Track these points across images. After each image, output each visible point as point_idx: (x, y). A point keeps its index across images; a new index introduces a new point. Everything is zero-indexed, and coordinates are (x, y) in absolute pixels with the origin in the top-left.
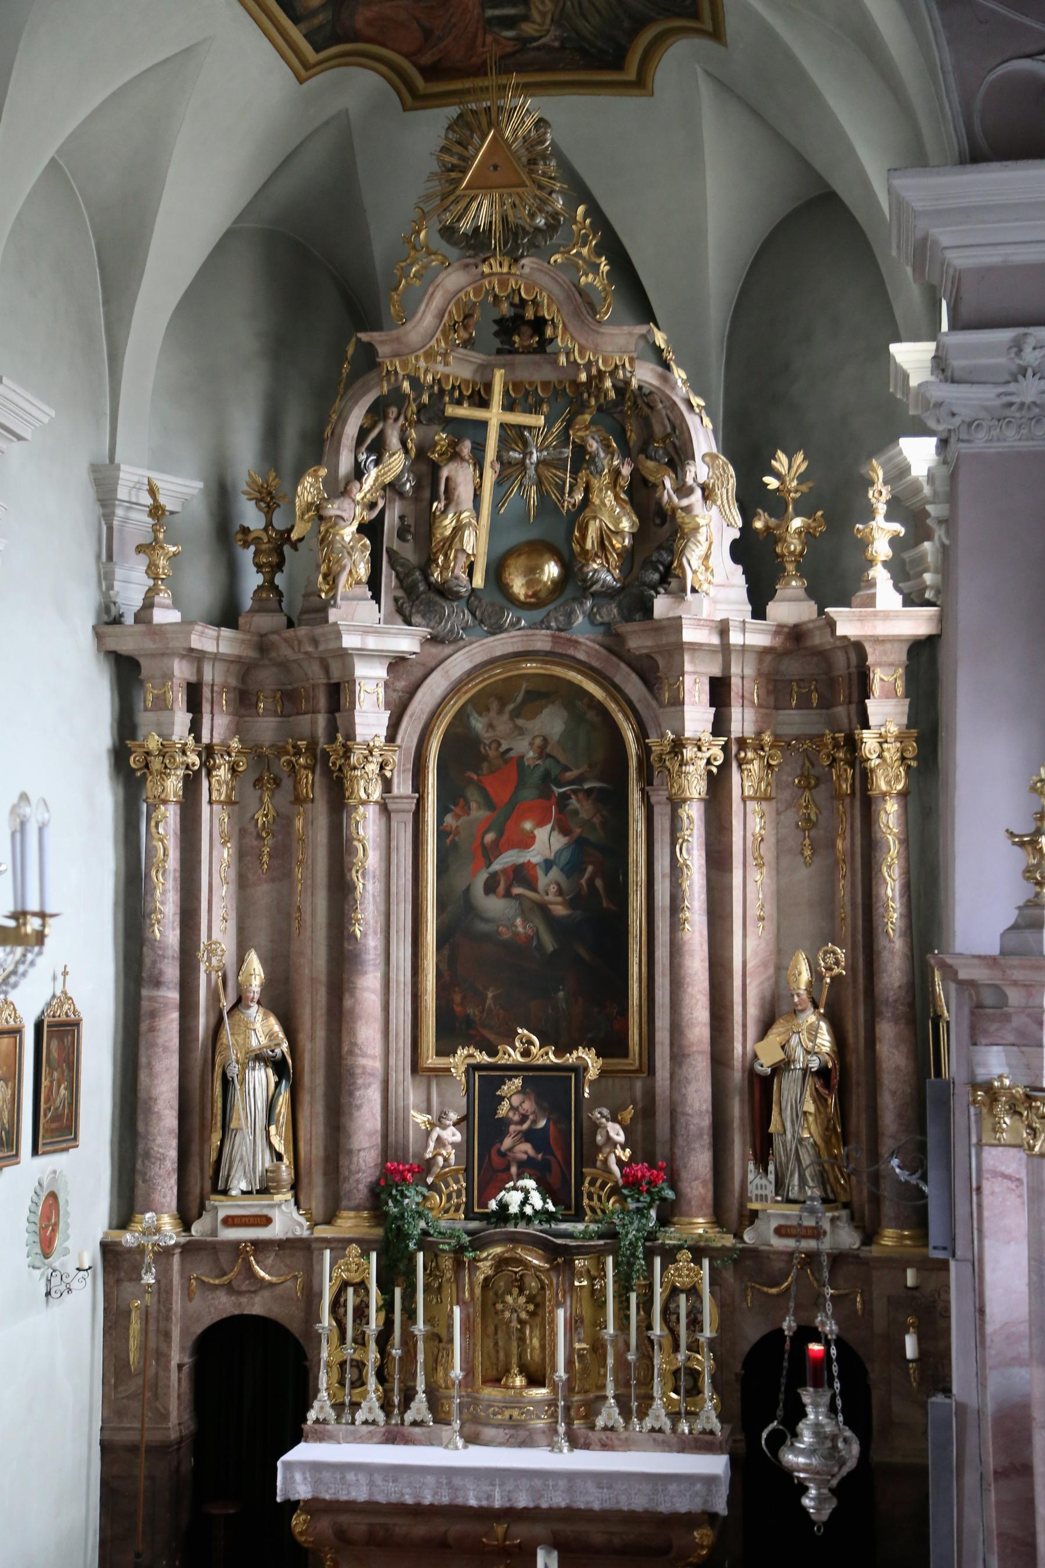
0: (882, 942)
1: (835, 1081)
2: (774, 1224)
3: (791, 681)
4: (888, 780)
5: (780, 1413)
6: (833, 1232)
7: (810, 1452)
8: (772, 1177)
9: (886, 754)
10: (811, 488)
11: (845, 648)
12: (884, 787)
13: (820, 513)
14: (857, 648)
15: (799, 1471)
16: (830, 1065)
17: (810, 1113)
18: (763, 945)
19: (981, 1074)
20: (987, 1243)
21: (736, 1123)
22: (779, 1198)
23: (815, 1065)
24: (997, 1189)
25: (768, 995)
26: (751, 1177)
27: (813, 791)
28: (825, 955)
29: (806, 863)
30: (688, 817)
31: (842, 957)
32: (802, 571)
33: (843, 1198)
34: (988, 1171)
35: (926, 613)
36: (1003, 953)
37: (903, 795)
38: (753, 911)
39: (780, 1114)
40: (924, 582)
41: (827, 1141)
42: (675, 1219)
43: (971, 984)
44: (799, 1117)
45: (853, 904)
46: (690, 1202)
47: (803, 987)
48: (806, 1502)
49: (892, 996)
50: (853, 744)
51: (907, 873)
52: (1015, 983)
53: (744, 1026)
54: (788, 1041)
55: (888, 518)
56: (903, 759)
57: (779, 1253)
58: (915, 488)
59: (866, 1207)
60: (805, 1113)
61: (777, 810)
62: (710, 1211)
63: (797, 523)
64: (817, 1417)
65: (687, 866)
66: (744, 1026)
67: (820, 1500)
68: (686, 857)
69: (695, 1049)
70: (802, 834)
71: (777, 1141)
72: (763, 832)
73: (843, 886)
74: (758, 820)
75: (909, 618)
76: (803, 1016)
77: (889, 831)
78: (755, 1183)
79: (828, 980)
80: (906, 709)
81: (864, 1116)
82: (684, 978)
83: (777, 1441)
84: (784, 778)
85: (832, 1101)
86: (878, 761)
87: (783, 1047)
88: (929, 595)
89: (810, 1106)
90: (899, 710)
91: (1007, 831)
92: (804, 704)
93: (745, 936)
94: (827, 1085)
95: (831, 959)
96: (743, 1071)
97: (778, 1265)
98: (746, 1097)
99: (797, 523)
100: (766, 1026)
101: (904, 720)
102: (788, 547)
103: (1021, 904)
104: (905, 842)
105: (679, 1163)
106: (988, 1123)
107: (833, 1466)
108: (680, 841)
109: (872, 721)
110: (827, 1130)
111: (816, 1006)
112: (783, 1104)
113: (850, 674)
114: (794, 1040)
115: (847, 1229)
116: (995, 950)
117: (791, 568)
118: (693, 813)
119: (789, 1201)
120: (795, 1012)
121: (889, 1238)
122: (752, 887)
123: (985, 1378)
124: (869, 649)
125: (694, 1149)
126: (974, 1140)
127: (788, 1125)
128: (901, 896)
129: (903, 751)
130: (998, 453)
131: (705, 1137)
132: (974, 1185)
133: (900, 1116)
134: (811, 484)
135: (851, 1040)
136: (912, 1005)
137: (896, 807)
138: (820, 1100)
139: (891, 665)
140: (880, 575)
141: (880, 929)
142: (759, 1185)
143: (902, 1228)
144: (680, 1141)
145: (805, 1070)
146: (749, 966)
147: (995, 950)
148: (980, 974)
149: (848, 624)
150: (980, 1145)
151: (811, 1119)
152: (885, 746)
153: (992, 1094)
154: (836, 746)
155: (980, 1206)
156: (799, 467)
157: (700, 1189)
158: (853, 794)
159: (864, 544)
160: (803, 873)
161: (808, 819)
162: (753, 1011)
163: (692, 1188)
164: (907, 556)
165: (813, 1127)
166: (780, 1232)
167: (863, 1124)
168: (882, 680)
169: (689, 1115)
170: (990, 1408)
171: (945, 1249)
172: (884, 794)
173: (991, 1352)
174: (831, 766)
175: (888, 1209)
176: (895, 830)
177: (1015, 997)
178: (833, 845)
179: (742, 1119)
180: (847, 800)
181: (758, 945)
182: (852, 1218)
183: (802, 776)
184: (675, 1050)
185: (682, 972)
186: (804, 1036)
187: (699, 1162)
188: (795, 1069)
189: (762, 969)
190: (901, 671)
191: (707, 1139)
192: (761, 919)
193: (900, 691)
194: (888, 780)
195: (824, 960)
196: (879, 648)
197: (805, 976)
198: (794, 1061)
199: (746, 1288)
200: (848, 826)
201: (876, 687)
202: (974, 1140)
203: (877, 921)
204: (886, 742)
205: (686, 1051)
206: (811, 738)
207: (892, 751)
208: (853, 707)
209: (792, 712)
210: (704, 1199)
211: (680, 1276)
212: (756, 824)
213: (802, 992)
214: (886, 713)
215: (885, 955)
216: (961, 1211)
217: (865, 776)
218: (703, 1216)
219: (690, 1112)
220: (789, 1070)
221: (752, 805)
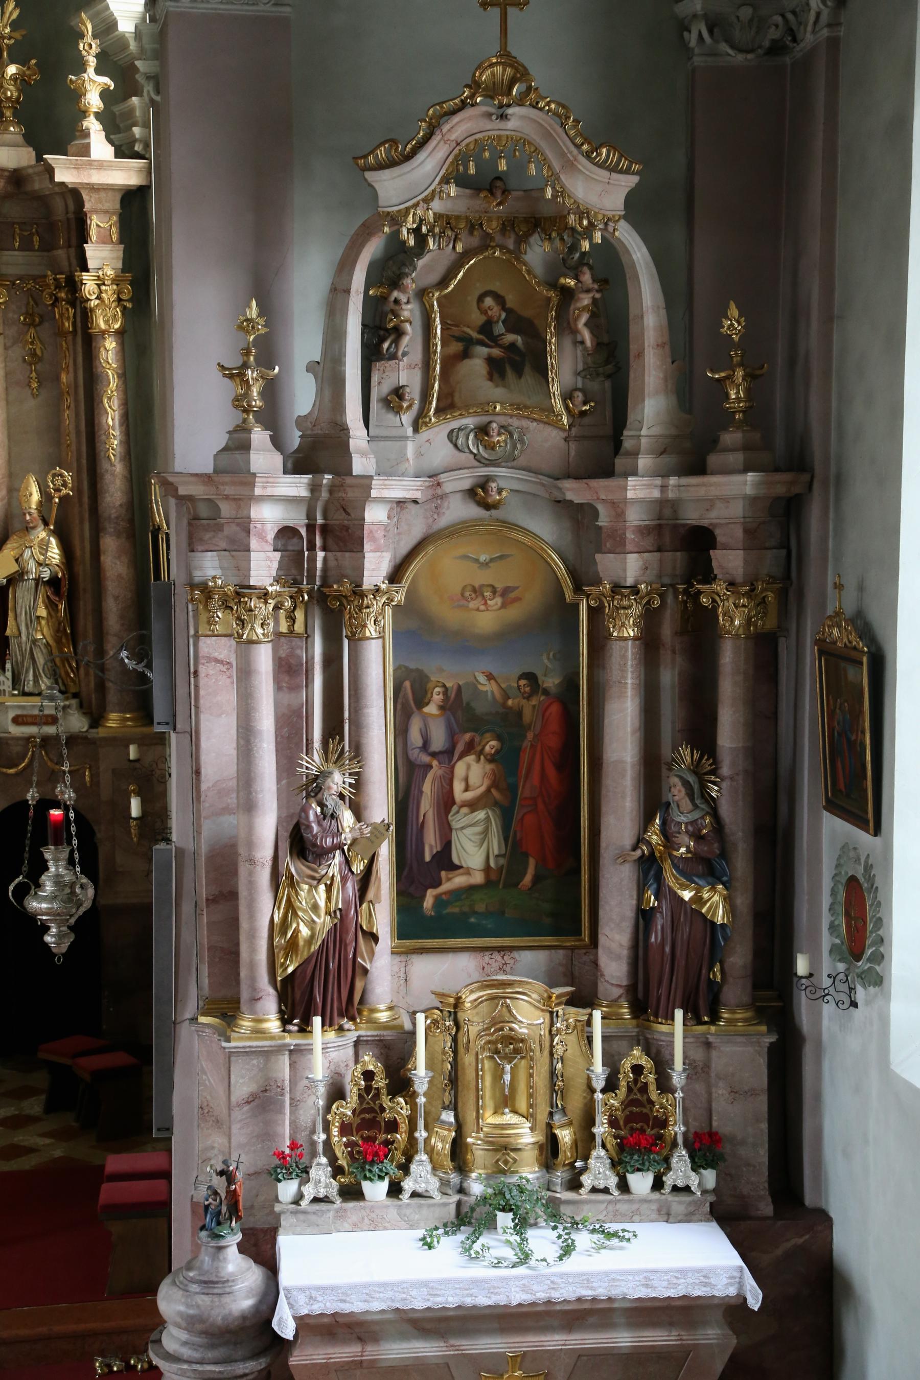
0: (105, 465)
1: (65, 589)
2: (11, 715)
3: (14, 223)
4: (107, 319)
5: (25, 869)
7: (52, 898)
8: (9, 674)
9: (104, 295)
10: (23, 36)
11: (62, 194)
12: (103, 326)
13: (33, 62)
14: (74, 194)
15: (42, 915)
16: (60, 575)
17: (43, 618)
19: (198, 576)
20: (203, 717)
22: (16, 692)
23: (46, 575)
24: (211, 672)
27: (38, 328)
29: (33, 395)
31: (69, 479)
32: (20, 118)
33: (73, 689)
34: (203, 657)
35: (136, 165)
36: (215, 471)
37: (120, 333)
39: (16, 619)
40: (134, 135)
41: (58, 641)
43: (190, 498)
45: (78, 432)
47: (34, 507)
48: (48, 939)
49: (114, 513)
50: (74, 286)
51: (125, 404)
52: (227, 497)
54: (21, 555)
55: (98, 71)
56: (119, 300)
58: (122, 41)
60: (38, 617)
61: (5, 345)
63: (12, 70)
64: (57, 869)
67: (60, 936)
70: (28, 367)
71: (13, 643)
73: (68, 416)
75: (121, 169)
76: (34, 532)
77: (108, 366)
79: (57, 500)
80: (121, 254)
83: (22, 892)
84: (11, 315)
85: (62, 607)
86: (97, 302)
87: (17, 560)
88: (138, 148)
89: (42, 612)
90: (115, 255)
91: (219, 364)
92: (26, 246)
94: (57, 592)
95: (59, 482)
97: (17, 749)
99: (12, 70)
101: (120, 265)
102: (5, 94)
103: (231, 429)
104: (123, 376)
106: (203, 617)
107: (72, 907)
109: (91, 264)
110: (58, 632)
111: (46, 524)
112: (18, 611)
113: (68, 219)
114: (27, 554)
115: (76, 715)
116: (209, 470)
117: (8, 113)
119: (25, 694)
120: (28, 529)
121: (113, 721)
123: (200, 826)
124: (85, 197)
126: (192, 632)
127: (23, 629)
128: (121, 425)
129: (119, 293)
130: (202, 13)
132: (192, 670)
133: (122, 617)
134: (24, 33)
135: (78, 553)
136: (131, 521)
137: (114, 345)
138: (51, 606)
139: (106, 212)
140: (93, 125)
141: (102, 454)
143: (125, 712)
145: (38, 580)
147: (209, 470)
148: (197, 490)
149: (65, 172)
150: (197, 636)
151: (43, 622)
152: (103, 288)
153: (207, 592)
154: (58, 287)
155: (196, 686)
156: (11, 13)
159: (78, 94)
160: (31, 403)
161: (33, 354)
164: (117, 109)
165: (45, 630)
166: (17, 721)
167: (90, 626)
168: (98, 226)
170: (204, 849)
171: (167, 724)
172: (103, 332)
173: (205, 805)
174: (53, 305)
175: (112, 697)
176: (114, 366)
177: (226, 509)
178: (58, 378)
180: (70, 338)
182: (81, 706)
183: (27, 314)
186: (36, 551)
188: (29, 579)
190: (115, 218)
193: (115, 237)
194: (107, 319)
195: (53, 482)
196: (95, 196)
197: (36, 497)
198: (27, 572)
201: (93, 233)
202: (192, 632)
203: (100, 447)
204: (104, 284)
206: (35, 278)
207: (110, 293)
208: (72, 251)
209: (16, 253)
213: (33, 511)
214: (102, 257)
215: (108, 477)
216: (181, 692)
217: (86, 315)
220: (23, 580)
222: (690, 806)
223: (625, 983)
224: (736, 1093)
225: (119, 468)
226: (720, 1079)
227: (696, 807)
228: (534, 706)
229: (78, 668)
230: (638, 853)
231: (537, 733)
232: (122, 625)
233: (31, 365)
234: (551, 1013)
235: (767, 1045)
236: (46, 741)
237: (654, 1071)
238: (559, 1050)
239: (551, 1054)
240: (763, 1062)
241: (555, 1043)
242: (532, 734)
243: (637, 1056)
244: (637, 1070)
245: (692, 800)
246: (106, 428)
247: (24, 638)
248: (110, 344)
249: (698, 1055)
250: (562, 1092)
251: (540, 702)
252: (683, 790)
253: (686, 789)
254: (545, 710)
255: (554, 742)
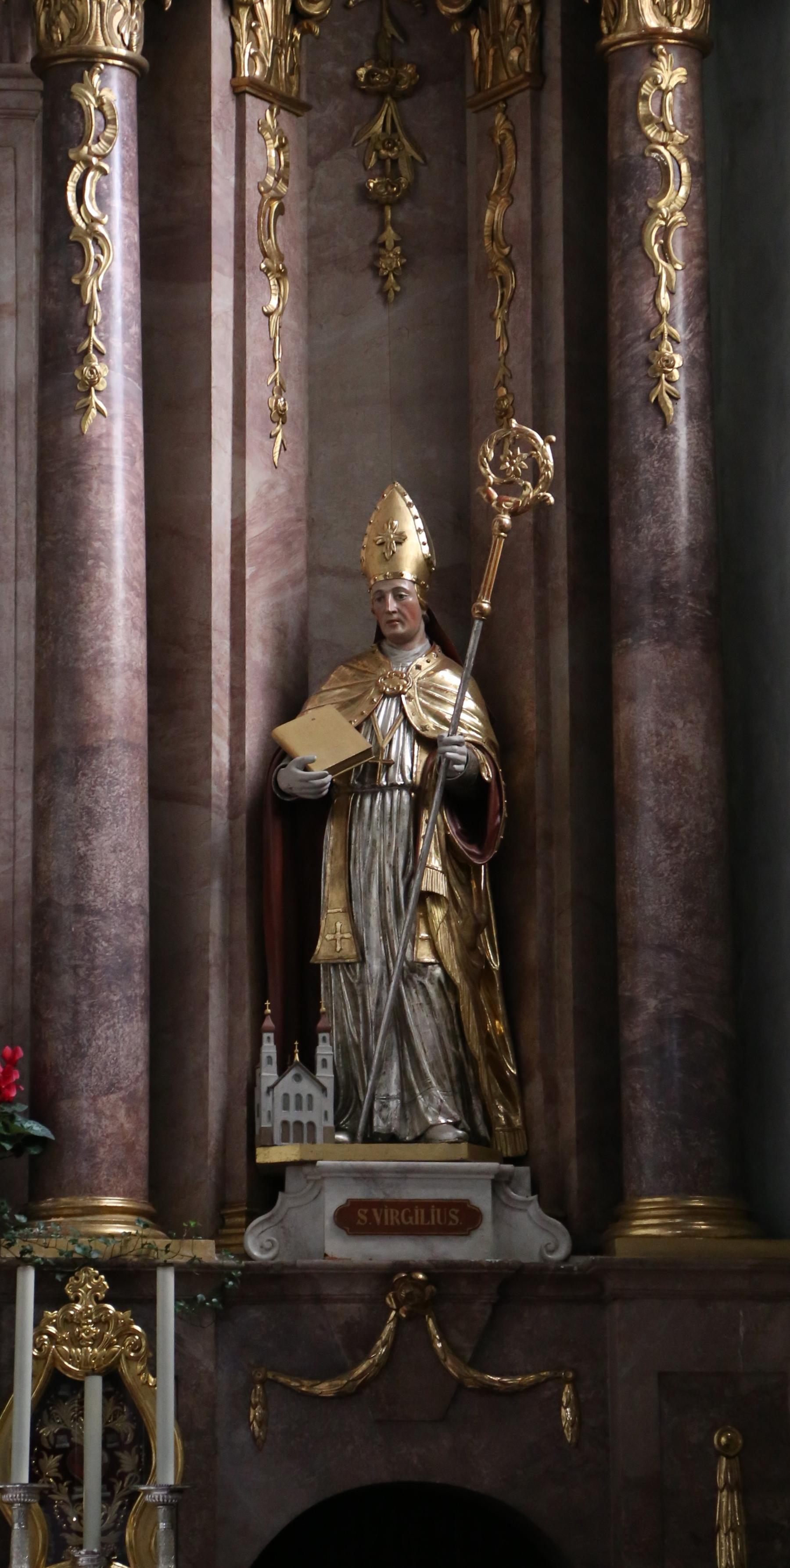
2: (334, 1200)
6: (496, 1218)
8: (325, 1075)
12: (652, 21)
17: (435, 898)
18: (281, 490)
21: (214, 951)
22: (341, 1137)
25: (292, 622)
26: (268, 1074)
27: (405, 104)
28: (499, 448)
29: (384, 293)
30: (100, 109)
31: (547, 454)
38: (259, 393)
39: (349, 911)
42: (48, 1203)
44: (397, 918)
45: (540, 370)
46: (92, 1152)
47: (408, 574)
53: (237, 692)
57: (348, 1273)
59: (573, 1166)
62: (141, 1183)
65: (97, 238)
66: (237, 692)
68: (95, 212)
69: (113, 734)
71: (334, 995)
72: (283, 189)
74: (273, 153)
77: (663, 137)
78: (279, 1091)
79: (507, 520)
81: (566, 921)
82: (86, 541)
89: (435, 877)
93: (239, 452)
96: (233, 816)
98: (242, 882)
100: (290, 702)
105: (57, 1048)
108: (77, 171)
112: (358, 882)
114: (386, 713)
115: (534, 1209)
118: (110, 91)
119: (371, 1137)
120: (385, 641)
121: (650, 1224)
122: (255, 321)
125: (106, 1006)
127: (374, 936)
128: (691, 312)
131: (137, 977)
135: (531, 722)
137: (680, 75)
138: (457, 865)
141: (636, 398)
142: (294, 1099)
143: (692, 1191)
144: (66, 984)
146: (252, 532)
151: (438, 914)
157: (121, 1114)
158: (537, 78)
160: (375, 320)
162: (258, 655)
163: (99, 1114)
165: (442, 939)
166: (351, 1219)
169: (98, 913)
172: (652, 37)
175: (649, 1143)
179: (228, 940)
180: (523, 99)
181: (272, 486)
184: (59, 738)
185: (83, 525)
187: (118, 1041)
188: (393, 786)
189: (277, 548)
191: (137, 985)
192: (281, 416)
195: (495, 466)
197: (415, 548)
198: (388, 765)
199: (251, 1383)
200: (525, 164)
205: (91, 740)
210: (130, 1148)
211: (76, 1341)
212: (265, 154)
213: (406, 586)
218: (127, 1194)
219: (99, 903)
220: (375, 789)
221: (258, 111)
225: (683, 438)
229: (522, 1079)
232: (689, 914)
233: (380, 206)
236: (443, 1274)
246: (653, 318)
247: (375, 965)
248: (671, 73)
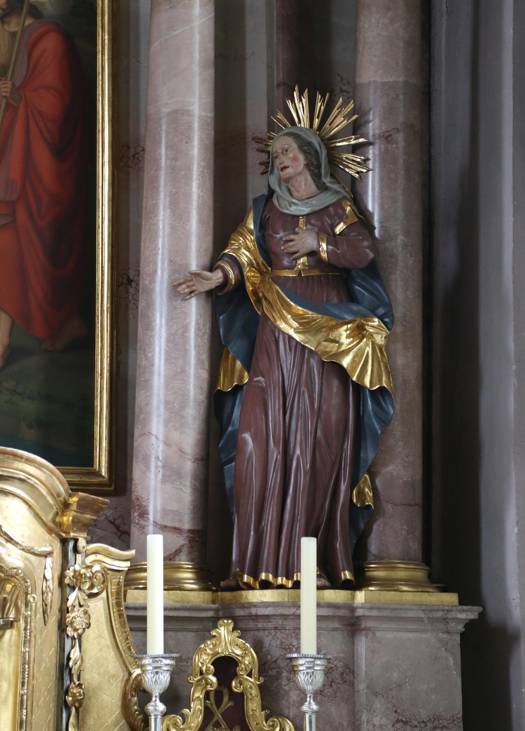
222: (313, 188)
223: (187, 526)
224: (406, 723)
226: (376, 694)
227: (322, 188)
228: (13, 35)
230: (217, 277)
231: (17, 84)
234: (64, 542)
235: (461, 628)
237: (255, 672)
238: (76, 616)
239: (62, 627)
240: (452, 661)
241: (69, 603)
242: (9, 85)
243: (226, 639)
244: (225, 666)
245: (316, 177)
249: (337, 644)
250: (77, 709)
251: (24, 29)
252: (301, 158)
253: (305, 153)
254: (35, 44)
255: (48, 103)
